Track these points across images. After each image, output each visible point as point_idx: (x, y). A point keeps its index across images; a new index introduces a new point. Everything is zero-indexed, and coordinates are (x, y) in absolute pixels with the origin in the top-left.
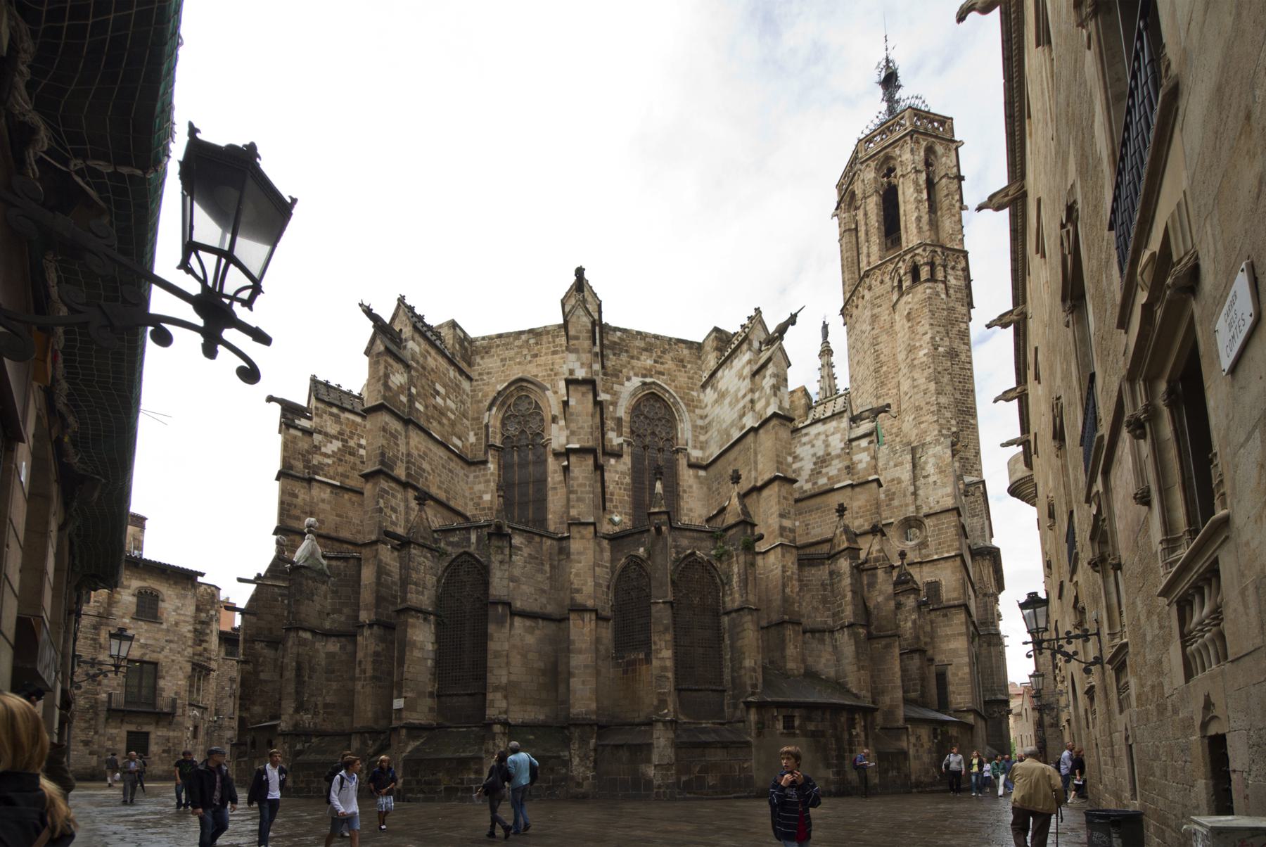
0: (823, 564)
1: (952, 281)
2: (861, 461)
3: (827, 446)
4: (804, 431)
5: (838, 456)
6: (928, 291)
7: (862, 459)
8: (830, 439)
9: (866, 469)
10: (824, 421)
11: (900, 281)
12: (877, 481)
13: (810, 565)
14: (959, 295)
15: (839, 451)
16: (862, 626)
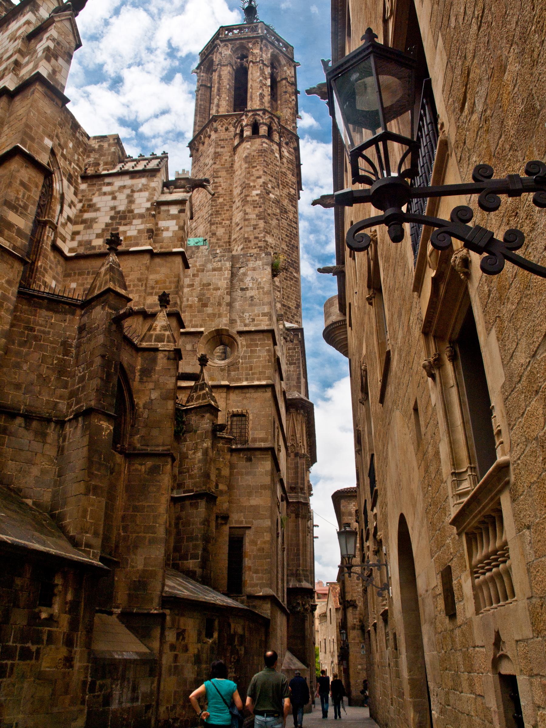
0: (73, 314)
1: (286, 154)
2: (167, 229)
3: (131, 200)
4: (107, 180)
5: (141, 216)
6: (264, 145)
7: (169, 227)
8: (136, 195)
10: (133, 174)
11: (242, 131)
12: (182, 254)
13: (48, 309)
14: (291, 167)
15: (143, 211)
16: (109, 418)
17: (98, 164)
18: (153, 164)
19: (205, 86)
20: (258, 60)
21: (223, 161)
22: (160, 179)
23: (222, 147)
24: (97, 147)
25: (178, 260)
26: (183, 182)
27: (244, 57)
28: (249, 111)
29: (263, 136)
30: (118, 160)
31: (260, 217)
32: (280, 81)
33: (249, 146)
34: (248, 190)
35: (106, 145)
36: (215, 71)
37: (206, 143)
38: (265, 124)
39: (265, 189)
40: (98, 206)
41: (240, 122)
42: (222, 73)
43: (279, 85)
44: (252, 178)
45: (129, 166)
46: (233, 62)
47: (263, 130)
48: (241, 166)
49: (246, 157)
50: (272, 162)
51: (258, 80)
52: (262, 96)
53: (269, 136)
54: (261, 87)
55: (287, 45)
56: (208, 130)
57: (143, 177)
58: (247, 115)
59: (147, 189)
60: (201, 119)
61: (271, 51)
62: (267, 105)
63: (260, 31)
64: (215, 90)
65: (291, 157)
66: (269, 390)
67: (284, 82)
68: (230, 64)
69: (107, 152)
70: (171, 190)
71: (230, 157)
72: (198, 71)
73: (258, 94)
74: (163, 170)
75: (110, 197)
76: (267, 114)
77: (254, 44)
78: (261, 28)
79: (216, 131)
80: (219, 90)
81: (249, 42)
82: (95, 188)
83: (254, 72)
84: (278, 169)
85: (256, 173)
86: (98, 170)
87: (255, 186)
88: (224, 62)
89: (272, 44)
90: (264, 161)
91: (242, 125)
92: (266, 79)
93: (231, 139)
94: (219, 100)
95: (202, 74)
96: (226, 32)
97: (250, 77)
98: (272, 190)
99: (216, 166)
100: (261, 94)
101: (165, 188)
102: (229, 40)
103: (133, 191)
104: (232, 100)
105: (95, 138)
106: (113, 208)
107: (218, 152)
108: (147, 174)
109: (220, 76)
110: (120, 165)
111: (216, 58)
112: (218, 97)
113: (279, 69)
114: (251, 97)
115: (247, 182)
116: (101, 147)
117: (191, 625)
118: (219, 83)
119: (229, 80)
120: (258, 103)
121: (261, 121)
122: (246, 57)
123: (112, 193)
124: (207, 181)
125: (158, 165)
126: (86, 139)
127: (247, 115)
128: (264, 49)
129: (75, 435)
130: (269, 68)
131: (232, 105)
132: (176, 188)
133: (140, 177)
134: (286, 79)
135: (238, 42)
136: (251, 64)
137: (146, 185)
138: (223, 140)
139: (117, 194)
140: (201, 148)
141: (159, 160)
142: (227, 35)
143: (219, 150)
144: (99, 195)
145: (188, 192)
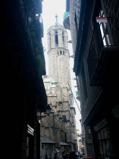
5: (49, 90)
9: (54, 94)
10: (47, 83)
11: (58, 52)
25: (55, 97)
27: (57, 33)
31: (63, 72)
47: (62, 53)
52: (61, 43)
64: (52, 41)
66: (68, 112)
99: (54, 59)
109: (52, 38)
117: (63, 148)
129: (51, 129)
143: (54, 56)
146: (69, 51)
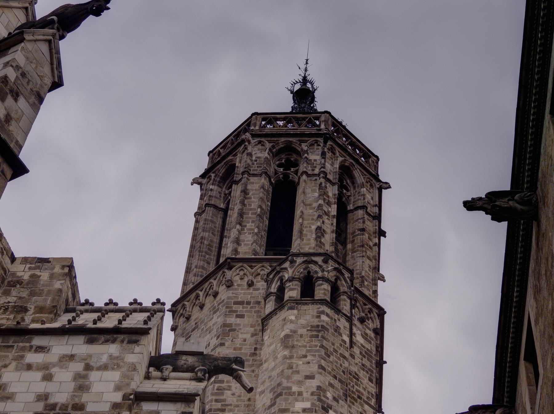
1: (359, 339)
3: (82, 385)
4: (37, 341)
6: (324, 318)
8: (94, 376)
10: (93, 334)
14: (368, 364)
17: (25, 310)
18: (136, 320)
19: (215, 207)
20: (317, 171)
21: (238, 342)
22: (147, 347)
23: (238, 316)
24: (26, 277)
26: (191, 360)
28: (298, 255)
29: (322, 302)
30: (63, 307)
32: (352, 211)
33: (293, 318)
34: (286, 400)
35: (44, 276)
36: (237, 183)
37: (208, 306)
38: (327, 280)
39: (320, 400)
40: (11, 389)
41: (278, 272)
42: (249, 187)
43: (350, 215)
44: (296, 377)
45: (86, 319)
46: (271, 171)
47: (322, 291)
48: (274, 351)
49: (287, 336)
50: (335, 351)
51: (315, 205)
52: (320, 232)
53: (333, 302)
54: (320, 216)
55: (368, 154)
56: (215, 283)
57: (113, 342)
58: (293, 262)
59: (119, 366)
60: (201, 263)
61: (340, 159)
62: (329, 248)
63: (323, 126)
64: (233, 215)
65: (368, 346)
67: (360, 212)
68: (266, 173)
69: (46, 289)
70: (166, 373)
71: (253, 335)
72: (204, 181)
73: (314, 227)
74: (153, 333)
75: (39, 375)
76: (331, 262)
77: (312, 145)
78: (326, 121)
79: (229, 285)
80: (241, 214)
81: (301, 142)
82: (11, 354)
83: (308, 191)
84: (346, 364)
85: (305, 370)
86: (23, 320)
87: (300, 394)
88: (255, 169)
89: (344, 149)
90: (322, 346)
91: (282, 280)
92: (329, 204)
93: (259, 303)
94: (240, 232)
95: (211, 187)
96: (263, 123)
97: (299, 198)
98: (334, 404)
100: (319, 228)
101: (151, 369)
102: (266, 136)
103: (88, 368)
104: (264, 234)
105: (25, 260)
106: (43, 397)
107: (230, 325)
108: (121, 337)
109: (245, 192)
110: (69, 316)
111: (241, 162)
112: (238, 227)
113: (352, 191)
114: (301, 232)
115: (285, 384)
116: (34, 278)
118: (243, 203)
119: (262, 199)
120: (313, 243)
121: (320, 275)
122: (296, 164)
123: (45, 367)
124: (239, 361)
125: (145, 322)
126: (7, 260)
127: (293, 262)
128: (329, 155)
130: (336, 187)
131: (264, 242)
132: (174, 370)
133: (106, 341)
134: (364, 207)
135: (283, 139)
136: (304, 177)
137: (117, 358)
138: (241, 303)
139: (54, 370)
140: (196, 314)
141: (148, 314)
142: (265, 126)
143: (232, 320)
144: (17, 369)
145: (200, 380)
146: (381, 313)
